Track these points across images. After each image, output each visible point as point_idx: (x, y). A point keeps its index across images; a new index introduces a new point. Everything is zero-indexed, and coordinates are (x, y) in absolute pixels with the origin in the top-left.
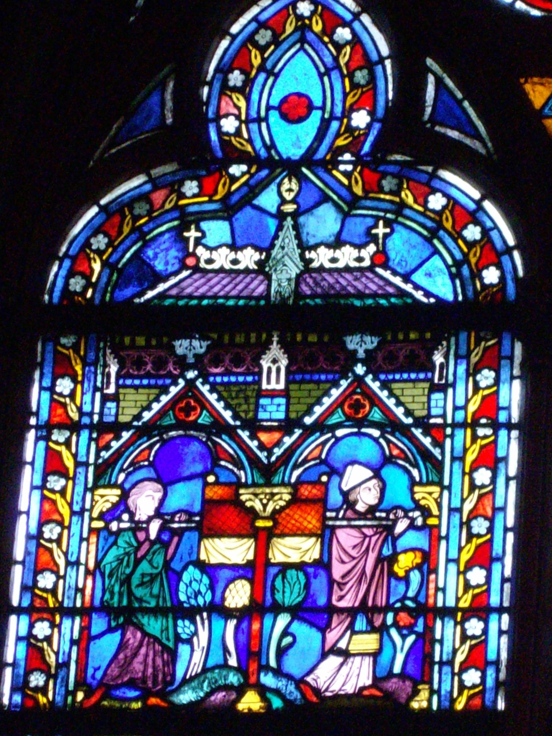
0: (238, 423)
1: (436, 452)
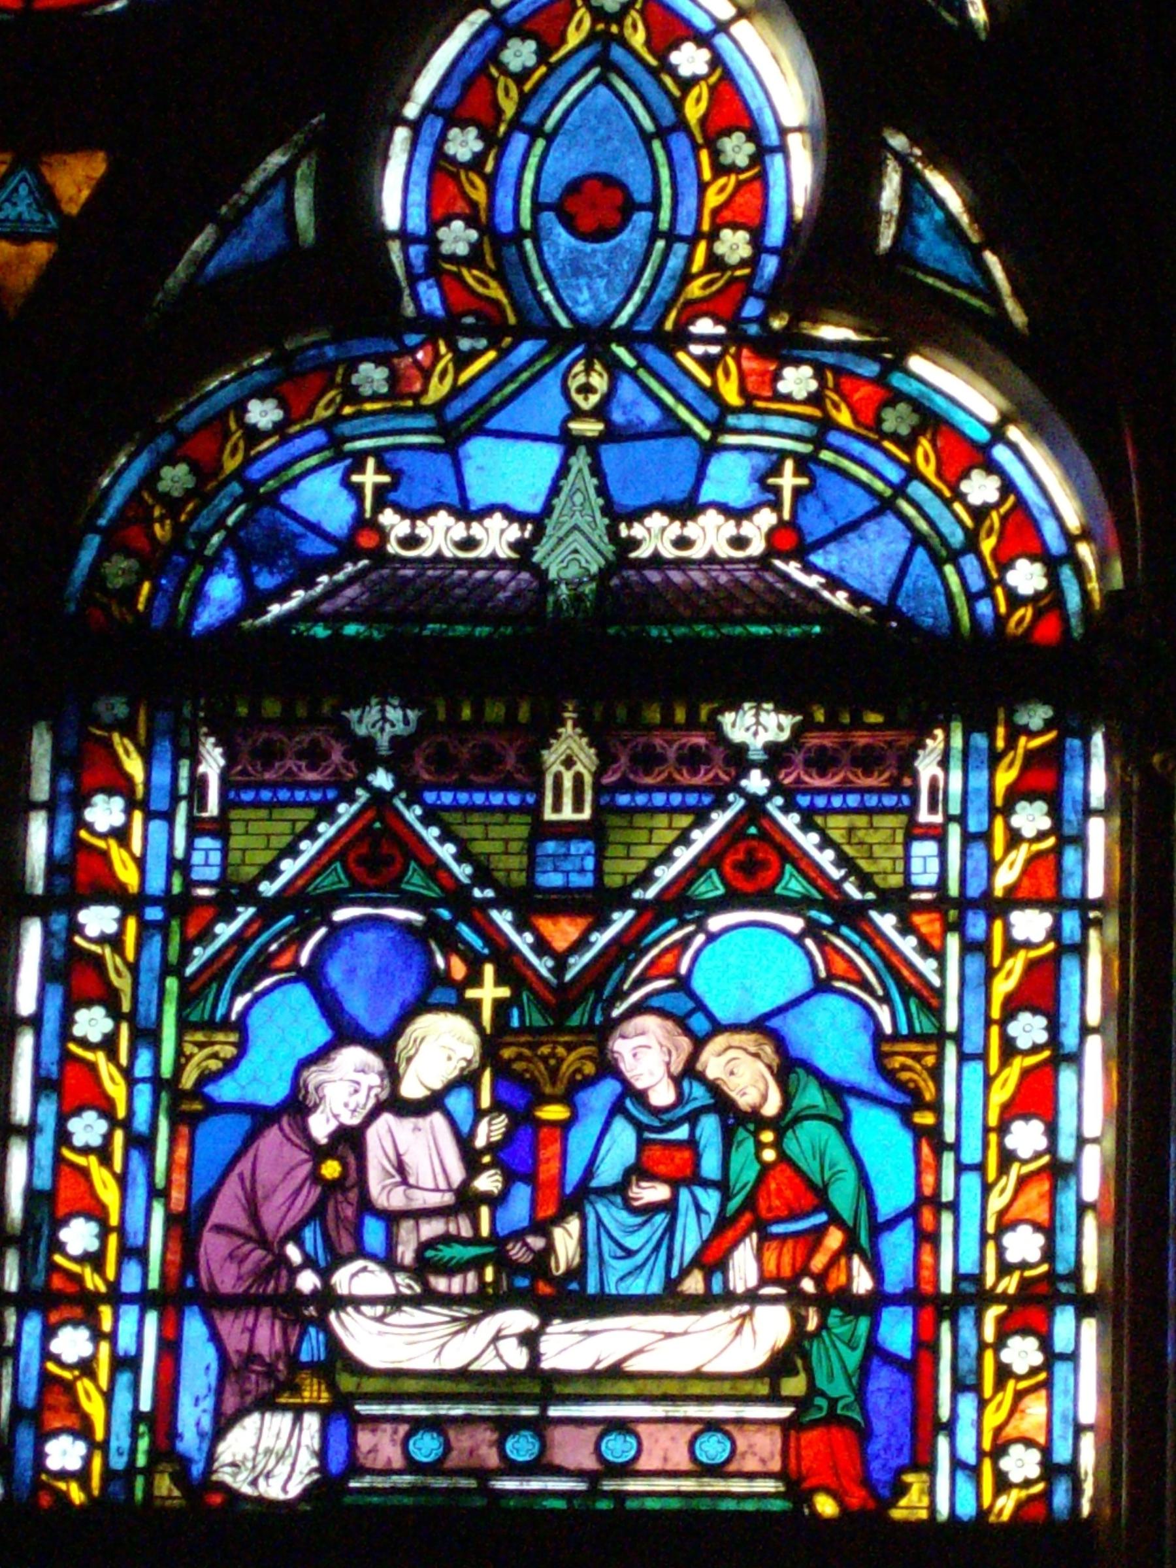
0: (870, 896)
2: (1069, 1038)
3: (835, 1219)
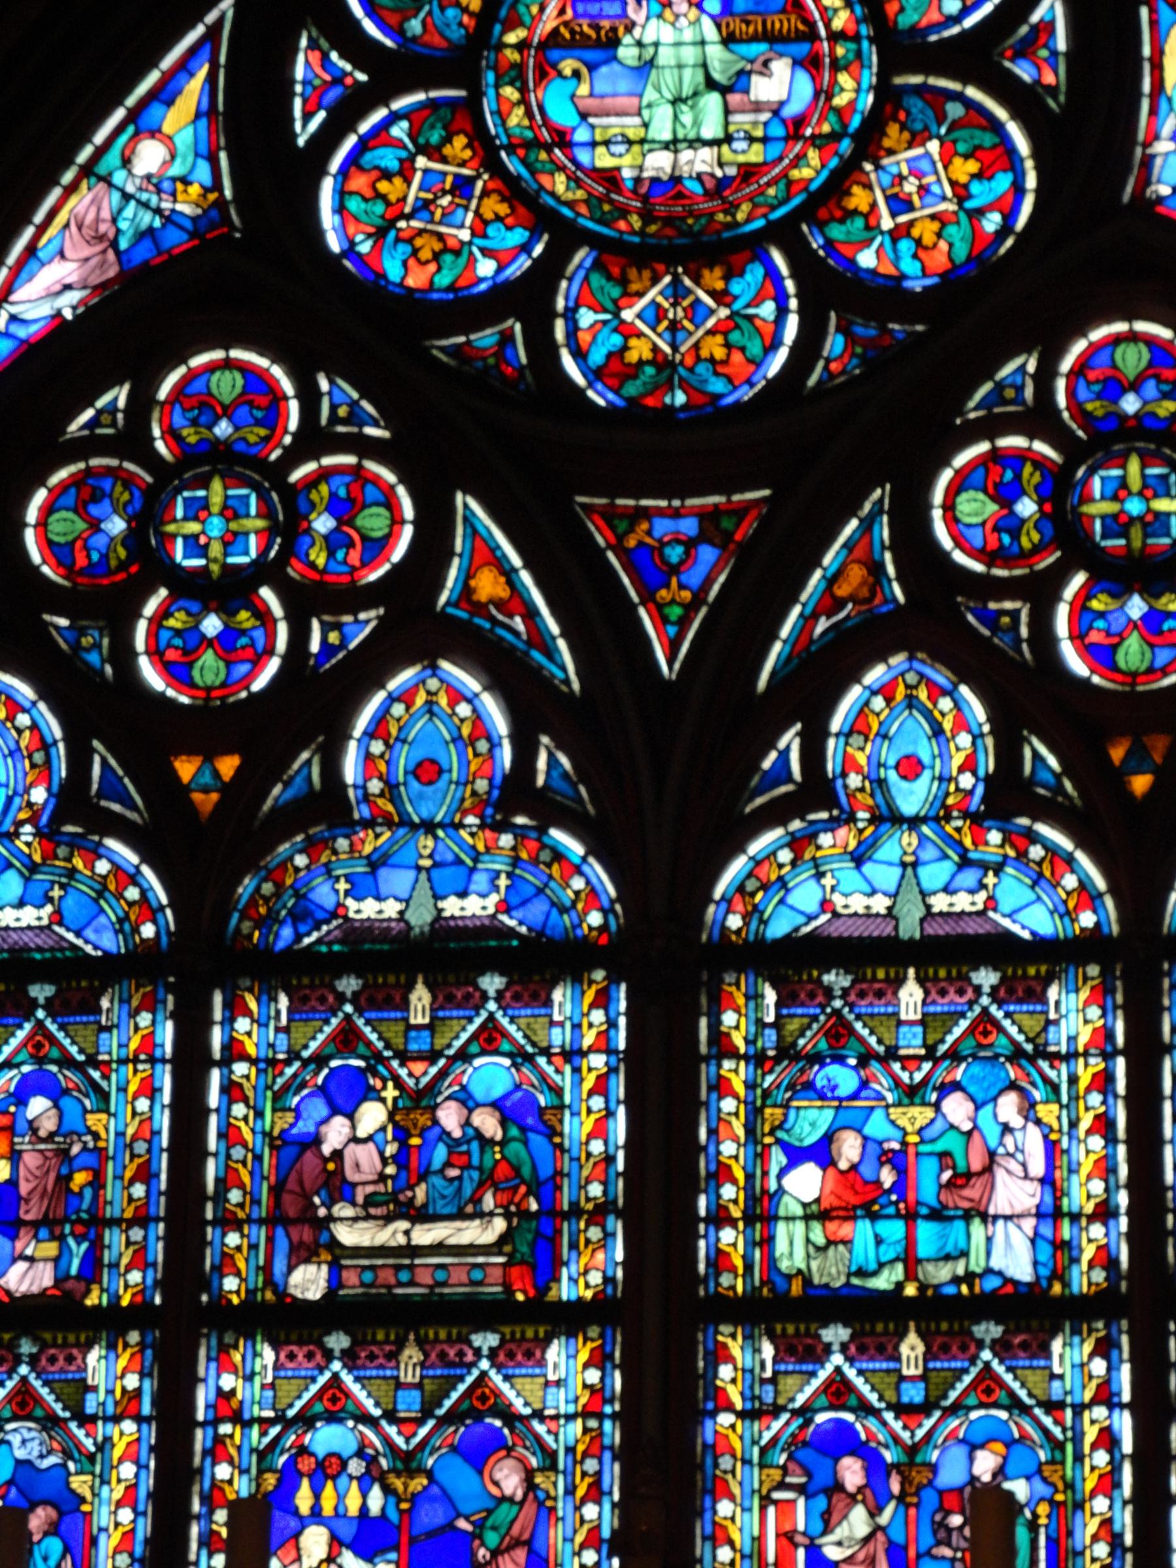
1: (104, 1084)
2: (612, 1105)
3: (523, 1182)
